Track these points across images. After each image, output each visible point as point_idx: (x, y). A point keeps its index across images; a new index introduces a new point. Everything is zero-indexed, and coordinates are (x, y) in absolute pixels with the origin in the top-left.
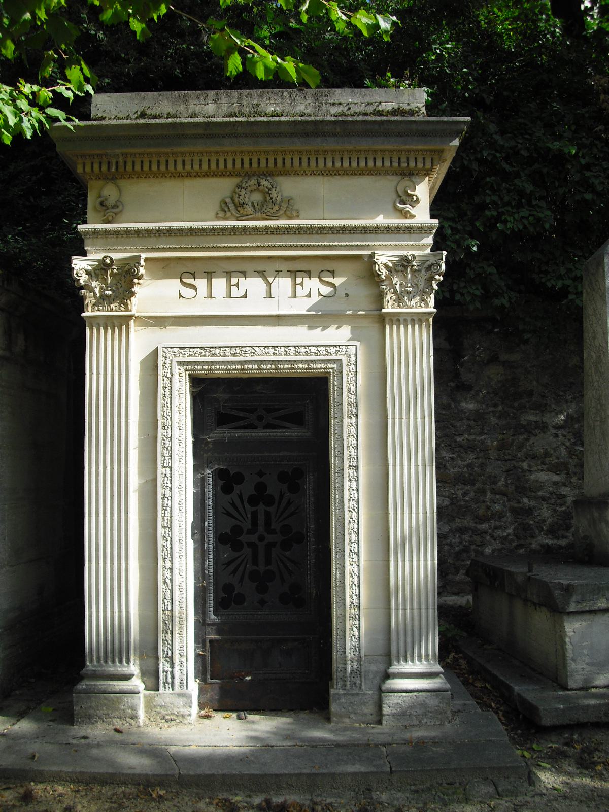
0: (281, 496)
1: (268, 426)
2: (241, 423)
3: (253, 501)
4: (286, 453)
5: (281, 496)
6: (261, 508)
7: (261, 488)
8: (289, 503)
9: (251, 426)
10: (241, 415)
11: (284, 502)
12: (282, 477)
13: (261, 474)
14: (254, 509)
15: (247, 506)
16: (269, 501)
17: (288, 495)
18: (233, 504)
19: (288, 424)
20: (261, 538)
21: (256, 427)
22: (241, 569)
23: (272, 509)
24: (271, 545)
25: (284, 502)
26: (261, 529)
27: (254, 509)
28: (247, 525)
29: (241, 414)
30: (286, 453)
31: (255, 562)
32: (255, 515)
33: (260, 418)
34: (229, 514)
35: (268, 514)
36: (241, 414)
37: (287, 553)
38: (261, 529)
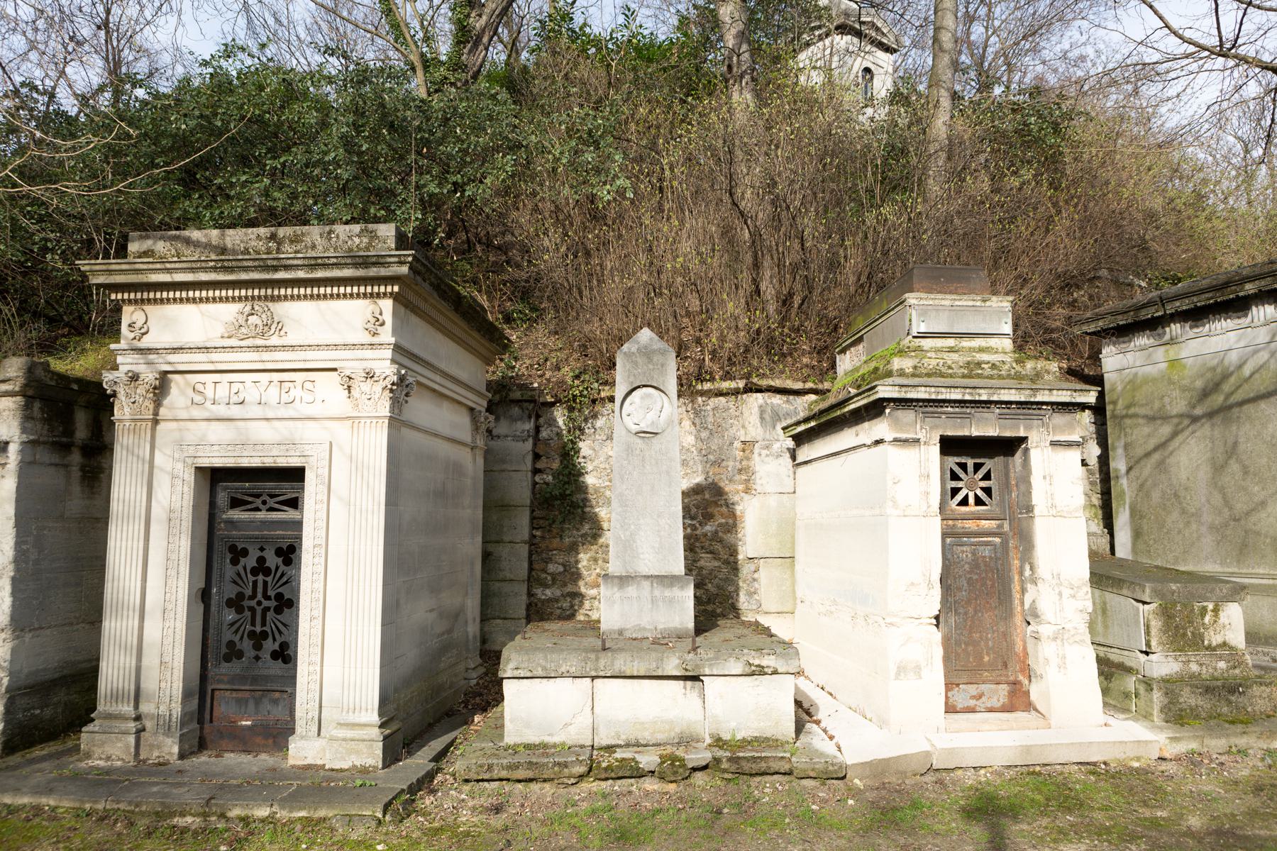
0: (277, 568)
1: (271, 509)
2: (249, 507)
3: (255, 572)
4: (281, 532)
5: (277, 568)
6: (261, 578)
7: (261, 560)
8: (283, 575)
9: (257, 509)
11: (278, 574)
12: (279, 552)
13: (262, 549)
14: (254, 578)
15: (249, 575)
16: (267, 572)
17: (282, 568)
18: (239, 575)
19: (285, 508)
20: (259, 603)
21: (260, 510)
22: (242, 628)
23: (269, 579)
24: (267, 609)
25: (278, 574)
26: (260, 596)
27: (254, 578)
28: (249, 592)
29: (250, 499)
30: (281, 532)
31: (253, 624)
32: (255, 583)
33: (264, 503)
34: (235, 582)
35: (265, 583)
36: (250, 499)
37: (278, 617)
38: (260, 596)
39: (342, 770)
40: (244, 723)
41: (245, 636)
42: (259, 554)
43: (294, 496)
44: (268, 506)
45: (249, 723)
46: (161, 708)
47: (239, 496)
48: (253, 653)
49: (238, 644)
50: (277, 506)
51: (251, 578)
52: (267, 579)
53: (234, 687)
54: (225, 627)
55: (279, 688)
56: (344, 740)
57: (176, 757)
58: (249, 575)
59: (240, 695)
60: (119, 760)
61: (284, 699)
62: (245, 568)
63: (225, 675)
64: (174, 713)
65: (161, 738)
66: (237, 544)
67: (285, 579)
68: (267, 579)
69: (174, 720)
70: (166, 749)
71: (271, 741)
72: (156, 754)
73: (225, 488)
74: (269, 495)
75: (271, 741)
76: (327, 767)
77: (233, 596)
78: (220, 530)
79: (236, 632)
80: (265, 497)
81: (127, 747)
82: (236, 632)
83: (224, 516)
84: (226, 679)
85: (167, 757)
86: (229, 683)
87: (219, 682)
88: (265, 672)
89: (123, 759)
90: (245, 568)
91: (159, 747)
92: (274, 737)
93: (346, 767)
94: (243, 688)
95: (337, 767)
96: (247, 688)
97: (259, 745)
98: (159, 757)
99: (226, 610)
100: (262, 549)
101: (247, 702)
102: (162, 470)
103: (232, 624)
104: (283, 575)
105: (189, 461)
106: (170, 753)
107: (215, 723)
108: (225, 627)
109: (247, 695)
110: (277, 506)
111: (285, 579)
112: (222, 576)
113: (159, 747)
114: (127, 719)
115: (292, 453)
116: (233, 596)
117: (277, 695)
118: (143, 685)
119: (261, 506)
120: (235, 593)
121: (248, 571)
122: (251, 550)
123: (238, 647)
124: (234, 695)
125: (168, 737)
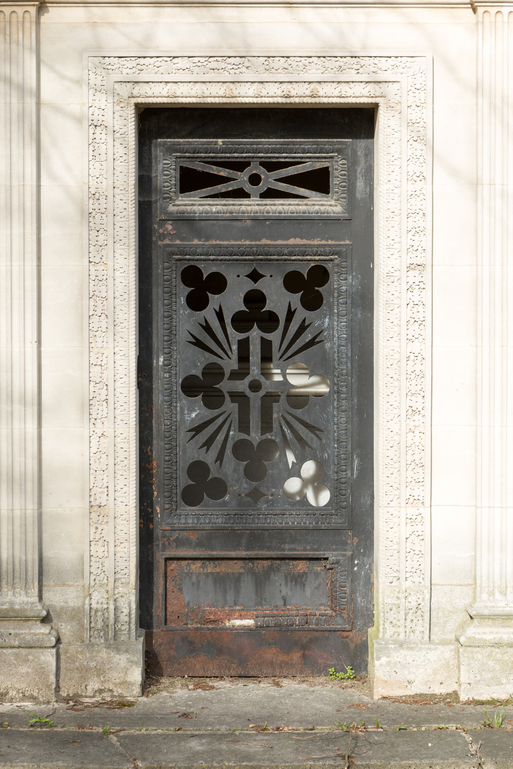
0: (290, 314)
2: (222, 188)
5: (290, 314)
8: (303, 328)
10: (222, 174)
13: (255, 276)
14: (242, 336)
15: (230, 329)
17: (301, 314)
18: (207, 328)
19: (302, 191)
21: (247, 196)
22: (221, 437)
23: (274, 337)
27: (242, 336)
29: (224, 172)
33: (255, 180)
34: (198, 343)
36: (224, 172)
37: (298, 412)
39: (492, 702)
40: (238, 623)
41: (228, 451)
42: (249, 285)
43: (318, 165)
44: (262, 187)
45: (249, 622)
46: (96, 596)
47: (199, 167)
48: (245, 486)
49: (213, 467)
50: (283, 187)
51: (235, 336)
52: (269, 336)
53: (215, 553)
54: (183, 436)
55: (311, 554)
56: (498, 645)
57: (137, 690)
58: (230, 329)
59: (223, 568)
60: (24, 698)
61: (317, 575)
62: (220, 315)
63: (194, 529)
64: (123, 603)
65: (104, 654)
66: (201, 266)
67: (307, 336)
68: (269, 336)
69: (123, 618)
70: (115, 676)
71: (296, 656)
72: (94, 685)
73: (171, 150)
74: (262, 164)
75: (296, 656)
76: (463, 697)
77: (197, 372)
78: (163, 237)
79: (208, 443)
80: (255, 169)
81: (41, 672)
82: (208, 443)
83: (171, 208)
84: (193, 537)
85: (118, 691)
86: (200, 544)
87: (180, 543)
88: (278, 523)
89: (33, 698)
90: (220, 315)
91: (100, 672)
92: (304, 648)
93: (503, 697)
94: (233, 554)
95: (485, 697)
96: (243, 554)
97: (272, 664)
98: (101, 691)
99: (184, 401)
100: (255, 276)
101: (238, 579)
102: (57, 109)
103: (198, 430)
104: (303, 328)
105: (124, 90)
106: (125, 684)
107: (172, 625)
108: (183, 436)
109: (237, 567)
110: (283, 187)
111: (307, 336)
112: (171, 331)
113: (100, 672)
114: (27, 619)
115: (351, 75)
116: (197, 372)
117: (301, 566)
118: (46, 554)
119: (248, 188)
120: (201, 366)
121: (228, 321)
122: (230, 277)
123: (214, 473)
124: (210, 568)
125: (118, 650)
